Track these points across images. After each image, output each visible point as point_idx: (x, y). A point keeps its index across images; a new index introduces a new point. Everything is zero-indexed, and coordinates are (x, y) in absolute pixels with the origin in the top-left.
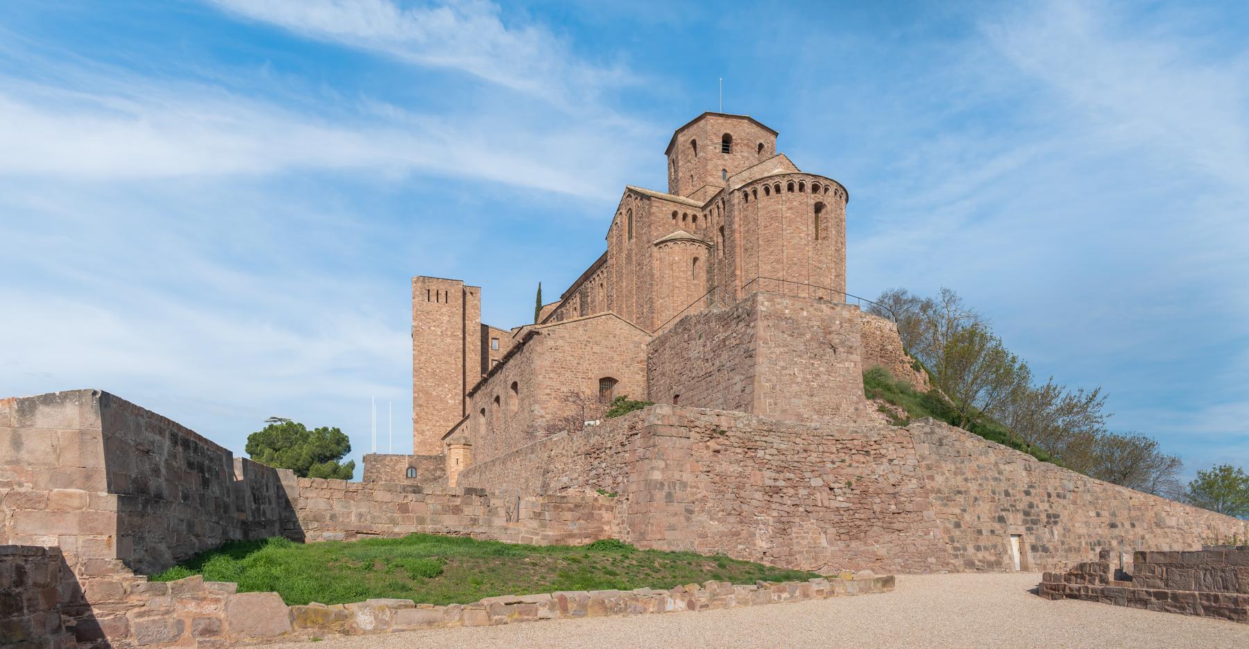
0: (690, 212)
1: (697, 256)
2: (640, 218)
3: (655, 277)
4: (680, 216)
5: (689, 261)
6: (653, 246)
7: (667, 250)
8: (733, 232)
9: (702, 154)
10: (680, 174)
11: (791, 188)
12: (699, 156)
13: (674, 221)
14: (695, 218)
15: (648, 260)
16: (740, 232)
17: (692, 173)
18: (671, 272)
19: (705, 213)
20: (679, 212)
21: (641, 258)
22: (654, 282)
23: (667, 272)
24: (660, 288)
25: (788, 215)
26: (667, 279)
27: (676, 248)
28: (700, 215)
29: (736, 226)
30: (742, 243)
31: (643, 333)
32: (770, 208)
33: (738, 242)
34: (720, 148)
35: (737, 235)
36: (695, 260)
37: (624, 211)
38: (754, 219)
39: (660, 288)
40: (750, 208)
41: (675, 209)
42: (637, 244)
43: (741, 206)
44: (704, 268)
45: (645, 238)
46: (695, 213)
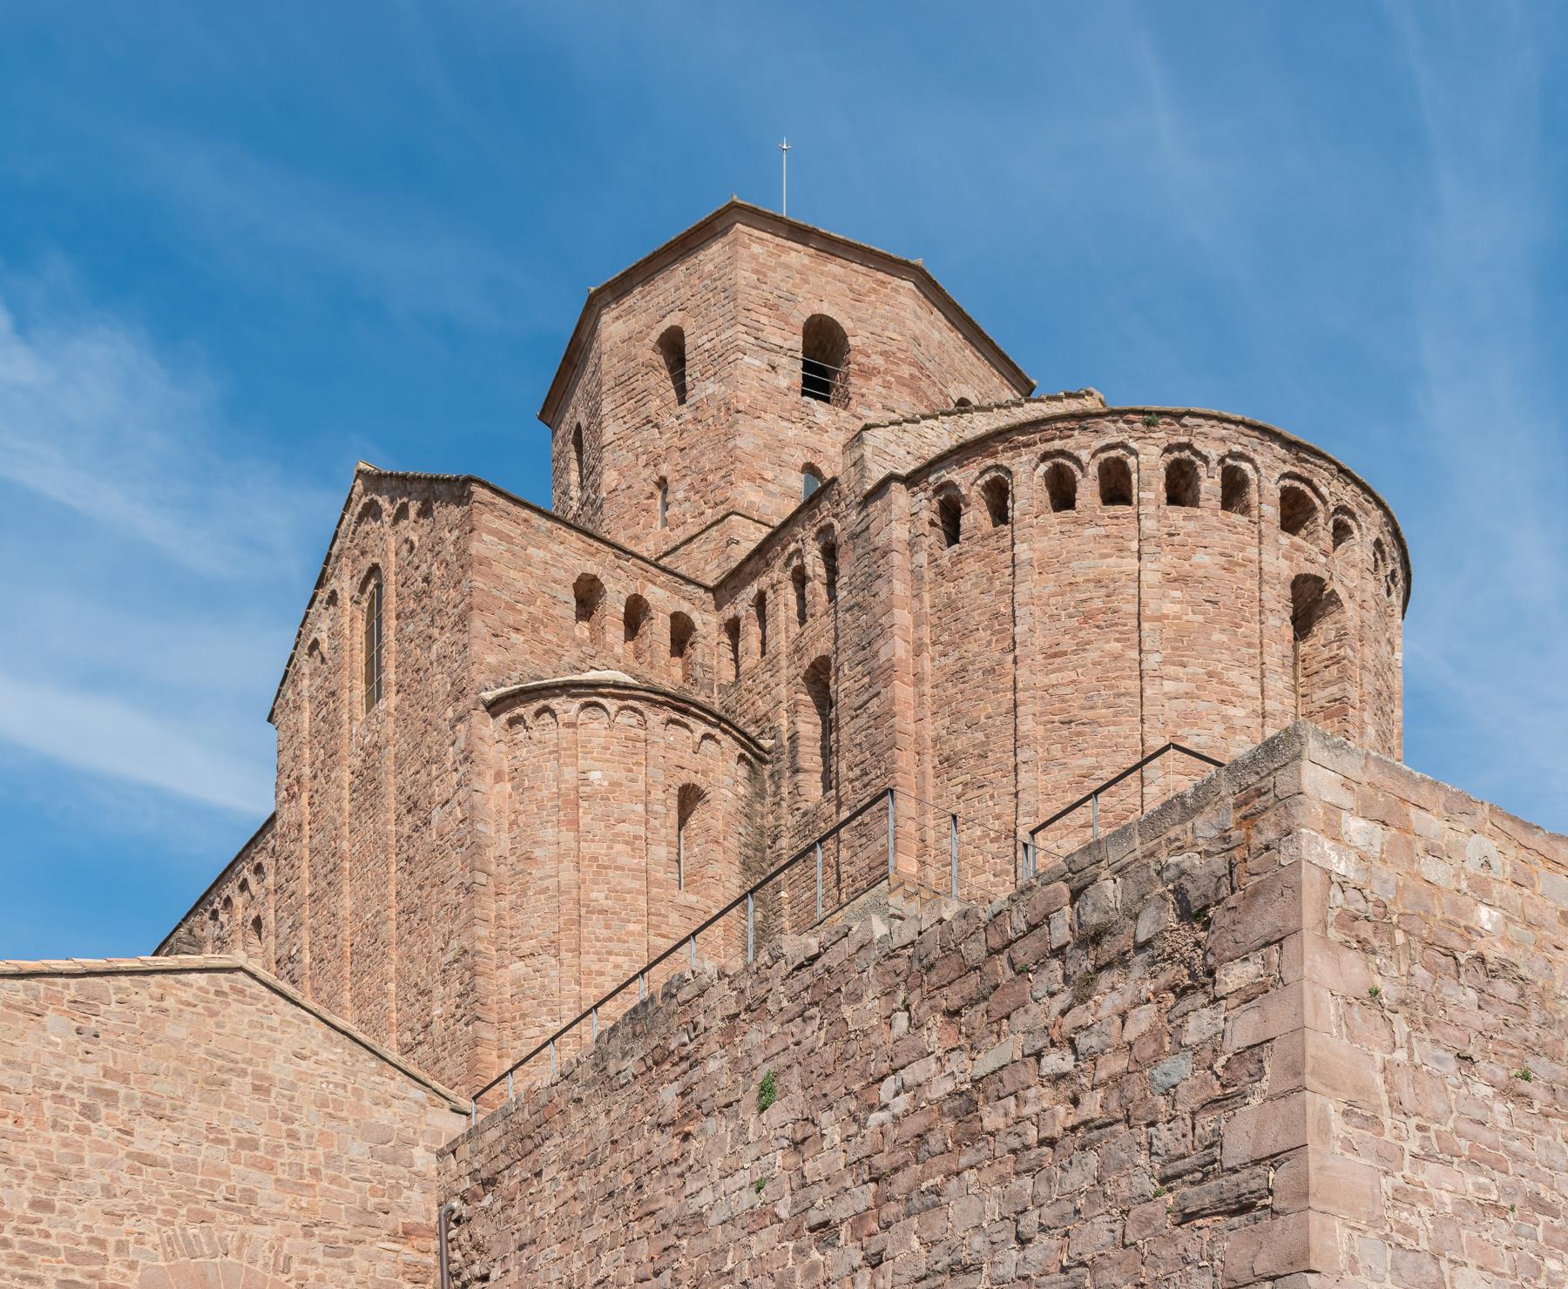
0: (662, 599)
1: (697, 780)
2: (418, 597)
3: (491, 853)
4: (613, 605)
5: (657, 794)
6: (480, 715)
7: (547, 732)
8: (879, 675)
9: (711, 387)
10: (610, 478)
11: (1180, 487)
12: (694, 396)
13: (583, 630)
14: (682, 632)
15: (456, 777)
16: (918, 678)
17: (665, 469)
18: (568, 837)
19: (729, 612)
20: (610, 586)
21: (423, 777)
22: (481, 878)
23: (549, 834)
24: (515, 908)
25: (1169, 608)
26: (549, 868)
27: (595, 727)
28: (707, 622)
29: (898, 648)
30: (930, 729)
31: (418, 1094)
32: (1082, 569)
33: (905, 722)
34: (791, 374)
35: (903, 691)
36: (689, 798)
37: (345, 584)
38: (996, 615)
39: (515, 908)
40: (971, 566)
41: (591, 567)
42: (403, 718)
43: (922, 558)
44: (732, 843)
45: (440, 682)
46: (685, 607)
